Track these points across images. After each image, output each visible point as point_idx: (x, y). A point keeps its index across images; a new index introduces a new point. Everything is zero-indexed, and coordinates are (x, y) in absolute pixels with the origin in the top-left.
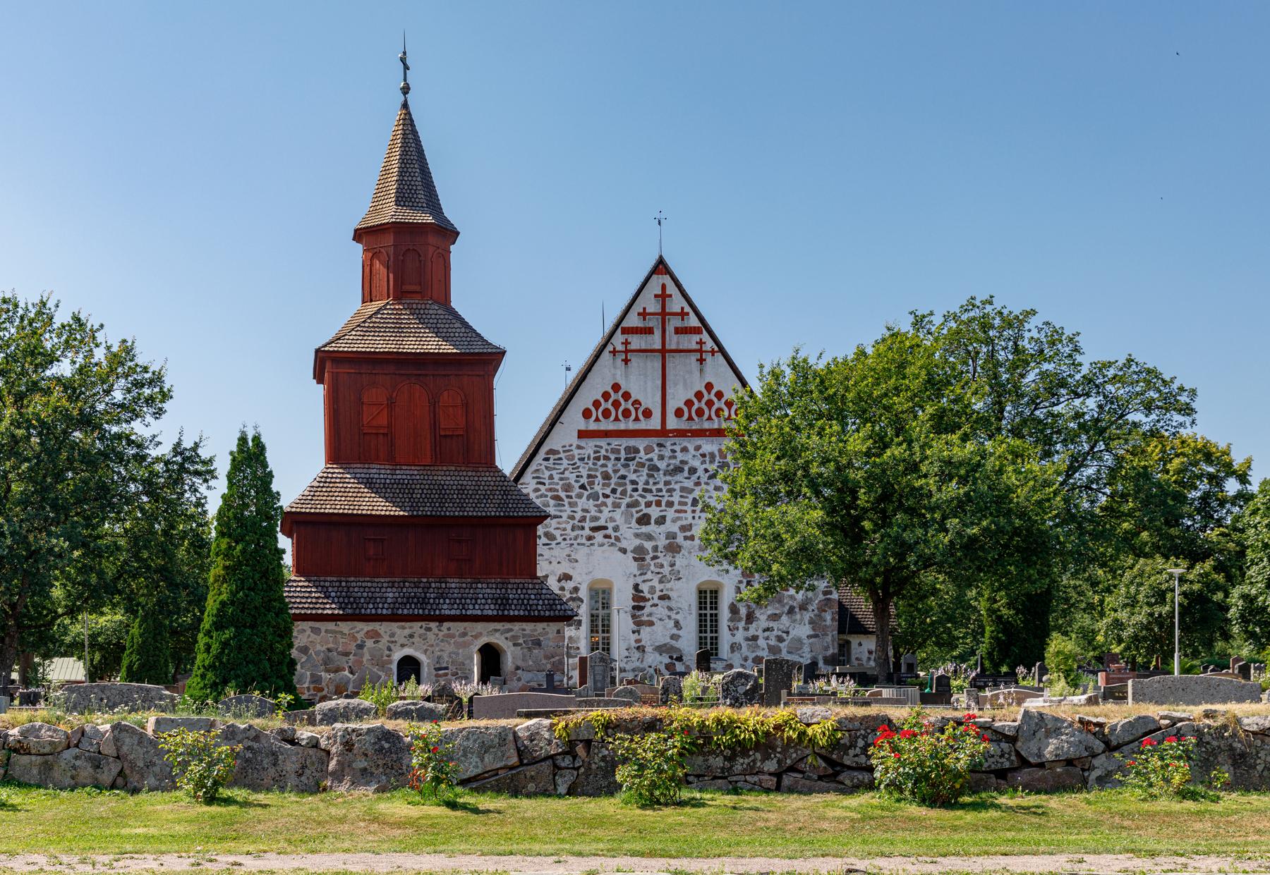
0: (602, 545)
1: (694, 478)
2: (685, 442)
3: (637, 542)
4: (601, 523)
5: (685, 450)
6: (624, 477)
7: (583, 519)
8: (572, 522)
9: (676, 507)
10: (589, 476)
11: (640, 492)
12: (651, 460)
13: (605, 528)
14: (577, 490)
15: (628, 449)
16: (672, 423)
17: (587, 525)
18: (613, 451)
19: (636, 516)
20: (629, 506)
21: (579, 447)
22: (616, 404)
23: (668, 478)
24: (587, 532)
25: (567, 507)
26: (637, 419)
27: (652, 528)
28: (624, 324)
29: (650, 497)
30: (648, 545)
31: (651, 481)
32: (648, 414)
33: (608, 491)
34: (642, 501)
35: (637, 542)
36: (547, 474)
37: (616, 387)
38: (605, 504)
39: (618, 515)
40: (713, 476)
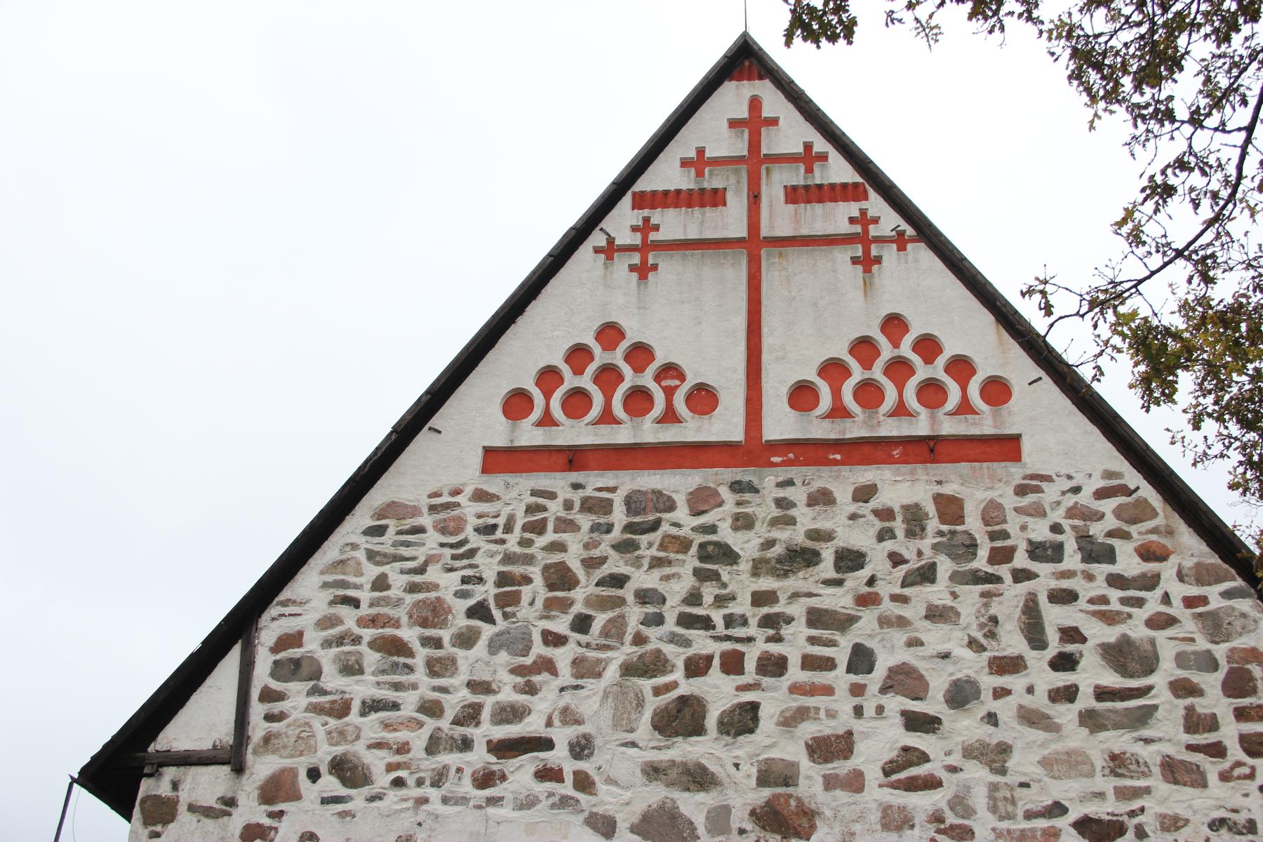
0: (528, 803)
1: (855, 581)
2: (822, 478)
3: (656, 793)
4: (532, 726)
5: (822, 499)
6: (618, 581)
7: (471, 715)
8: (430, 724)
9: (795, 673)
10: (503, 580)
11: (670, 625)
12: (712, 529)
13: (547, 744)
14: (461, 622)
15: (633, 503)
16: (781, 423)
17: (487, 731)
18: (588, 506)
19: (653, 703)
20: (629, 670)
21: (481, 496)
22: (607, 377)
23: (766, 583)
24: (479, 757)
25: (420, 675)
26: (670, 416)
27: (704, 749)
28: (646, 183)
29: (702, 643)
30: (694, 806)
31: (709, 592)
32: (703, 399)
33: (561, 625)
34: (677, 656)
35: (656, 793)
36: (372, 571)
37: (610, 333)
38: (548, 666)
39: (592, 702)
40: (926, 575)
